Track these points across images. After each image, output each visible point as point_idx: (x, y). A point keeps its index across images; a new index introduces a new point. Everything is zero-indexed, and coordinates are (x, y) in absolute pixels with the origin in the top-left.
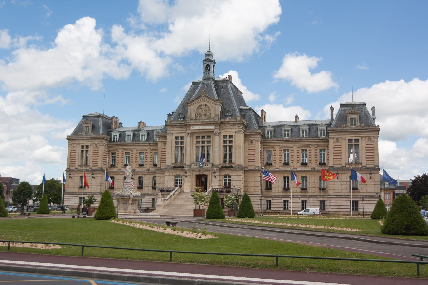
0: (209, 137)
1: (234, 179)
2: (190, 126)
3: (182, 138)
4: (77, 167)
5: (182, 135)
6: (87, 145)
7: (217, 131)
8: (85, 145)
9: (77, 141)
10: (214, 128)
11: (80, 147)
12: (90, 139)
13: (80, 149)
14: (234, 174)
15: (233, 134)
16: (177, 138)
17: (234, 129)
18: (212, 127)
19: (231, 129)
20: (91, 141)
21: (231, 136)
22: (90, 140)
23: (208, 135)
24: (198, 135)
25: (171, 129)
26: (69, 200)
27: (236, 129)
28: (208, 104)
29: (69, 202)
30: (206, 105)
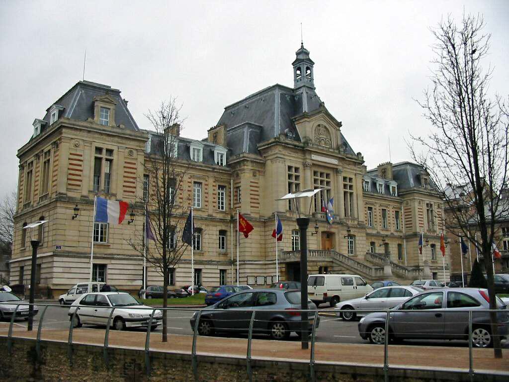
0: (328, 176)
1: (359, 242)
2: (311, 152)
3: (297, 169)
4: (85, 193)
5: (297, 166)
6: (110, 147)
7: (340, 168)
8: (105, 147)
9: (85, 134)
10: (337, 163)
11: (94, 149)
12: (119, 137)
13: (94, 154)
14: (359, 235)
15: (353, 176)
16: (290, 168)
17: (354, 170)
18: (335, 162)
19: (351, 169)
20: (120, 140)
21: (350, 179)
22: (116, 139)
23: (328, 172)
24: (316, 169)
25: (283, 153)
26: (67, 270)
27: (356, 170)
28: (328, 127)
29: (66, 275)
30: (325, 127)
